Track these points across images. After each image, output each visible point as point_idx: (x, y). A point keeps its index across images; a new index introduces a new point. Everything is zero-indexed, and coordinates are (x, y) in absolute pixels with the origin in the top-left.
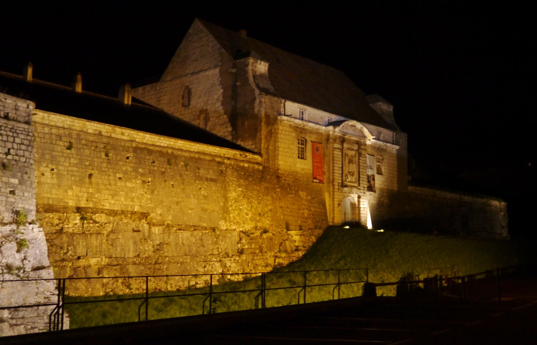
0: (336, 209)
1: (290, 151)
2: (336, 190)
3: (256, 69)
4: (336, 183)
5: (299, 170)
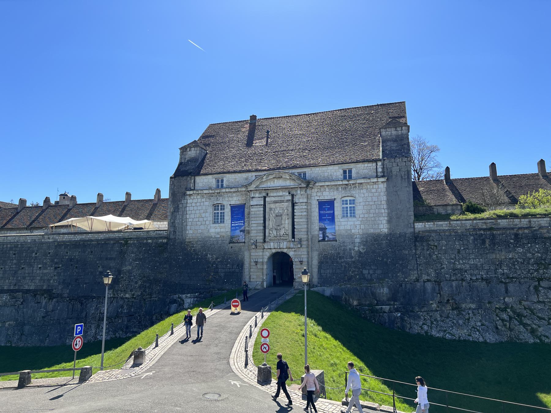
0: (252, 267)
1: (201, 219)
3: (187, 157)
5: (213, 235)
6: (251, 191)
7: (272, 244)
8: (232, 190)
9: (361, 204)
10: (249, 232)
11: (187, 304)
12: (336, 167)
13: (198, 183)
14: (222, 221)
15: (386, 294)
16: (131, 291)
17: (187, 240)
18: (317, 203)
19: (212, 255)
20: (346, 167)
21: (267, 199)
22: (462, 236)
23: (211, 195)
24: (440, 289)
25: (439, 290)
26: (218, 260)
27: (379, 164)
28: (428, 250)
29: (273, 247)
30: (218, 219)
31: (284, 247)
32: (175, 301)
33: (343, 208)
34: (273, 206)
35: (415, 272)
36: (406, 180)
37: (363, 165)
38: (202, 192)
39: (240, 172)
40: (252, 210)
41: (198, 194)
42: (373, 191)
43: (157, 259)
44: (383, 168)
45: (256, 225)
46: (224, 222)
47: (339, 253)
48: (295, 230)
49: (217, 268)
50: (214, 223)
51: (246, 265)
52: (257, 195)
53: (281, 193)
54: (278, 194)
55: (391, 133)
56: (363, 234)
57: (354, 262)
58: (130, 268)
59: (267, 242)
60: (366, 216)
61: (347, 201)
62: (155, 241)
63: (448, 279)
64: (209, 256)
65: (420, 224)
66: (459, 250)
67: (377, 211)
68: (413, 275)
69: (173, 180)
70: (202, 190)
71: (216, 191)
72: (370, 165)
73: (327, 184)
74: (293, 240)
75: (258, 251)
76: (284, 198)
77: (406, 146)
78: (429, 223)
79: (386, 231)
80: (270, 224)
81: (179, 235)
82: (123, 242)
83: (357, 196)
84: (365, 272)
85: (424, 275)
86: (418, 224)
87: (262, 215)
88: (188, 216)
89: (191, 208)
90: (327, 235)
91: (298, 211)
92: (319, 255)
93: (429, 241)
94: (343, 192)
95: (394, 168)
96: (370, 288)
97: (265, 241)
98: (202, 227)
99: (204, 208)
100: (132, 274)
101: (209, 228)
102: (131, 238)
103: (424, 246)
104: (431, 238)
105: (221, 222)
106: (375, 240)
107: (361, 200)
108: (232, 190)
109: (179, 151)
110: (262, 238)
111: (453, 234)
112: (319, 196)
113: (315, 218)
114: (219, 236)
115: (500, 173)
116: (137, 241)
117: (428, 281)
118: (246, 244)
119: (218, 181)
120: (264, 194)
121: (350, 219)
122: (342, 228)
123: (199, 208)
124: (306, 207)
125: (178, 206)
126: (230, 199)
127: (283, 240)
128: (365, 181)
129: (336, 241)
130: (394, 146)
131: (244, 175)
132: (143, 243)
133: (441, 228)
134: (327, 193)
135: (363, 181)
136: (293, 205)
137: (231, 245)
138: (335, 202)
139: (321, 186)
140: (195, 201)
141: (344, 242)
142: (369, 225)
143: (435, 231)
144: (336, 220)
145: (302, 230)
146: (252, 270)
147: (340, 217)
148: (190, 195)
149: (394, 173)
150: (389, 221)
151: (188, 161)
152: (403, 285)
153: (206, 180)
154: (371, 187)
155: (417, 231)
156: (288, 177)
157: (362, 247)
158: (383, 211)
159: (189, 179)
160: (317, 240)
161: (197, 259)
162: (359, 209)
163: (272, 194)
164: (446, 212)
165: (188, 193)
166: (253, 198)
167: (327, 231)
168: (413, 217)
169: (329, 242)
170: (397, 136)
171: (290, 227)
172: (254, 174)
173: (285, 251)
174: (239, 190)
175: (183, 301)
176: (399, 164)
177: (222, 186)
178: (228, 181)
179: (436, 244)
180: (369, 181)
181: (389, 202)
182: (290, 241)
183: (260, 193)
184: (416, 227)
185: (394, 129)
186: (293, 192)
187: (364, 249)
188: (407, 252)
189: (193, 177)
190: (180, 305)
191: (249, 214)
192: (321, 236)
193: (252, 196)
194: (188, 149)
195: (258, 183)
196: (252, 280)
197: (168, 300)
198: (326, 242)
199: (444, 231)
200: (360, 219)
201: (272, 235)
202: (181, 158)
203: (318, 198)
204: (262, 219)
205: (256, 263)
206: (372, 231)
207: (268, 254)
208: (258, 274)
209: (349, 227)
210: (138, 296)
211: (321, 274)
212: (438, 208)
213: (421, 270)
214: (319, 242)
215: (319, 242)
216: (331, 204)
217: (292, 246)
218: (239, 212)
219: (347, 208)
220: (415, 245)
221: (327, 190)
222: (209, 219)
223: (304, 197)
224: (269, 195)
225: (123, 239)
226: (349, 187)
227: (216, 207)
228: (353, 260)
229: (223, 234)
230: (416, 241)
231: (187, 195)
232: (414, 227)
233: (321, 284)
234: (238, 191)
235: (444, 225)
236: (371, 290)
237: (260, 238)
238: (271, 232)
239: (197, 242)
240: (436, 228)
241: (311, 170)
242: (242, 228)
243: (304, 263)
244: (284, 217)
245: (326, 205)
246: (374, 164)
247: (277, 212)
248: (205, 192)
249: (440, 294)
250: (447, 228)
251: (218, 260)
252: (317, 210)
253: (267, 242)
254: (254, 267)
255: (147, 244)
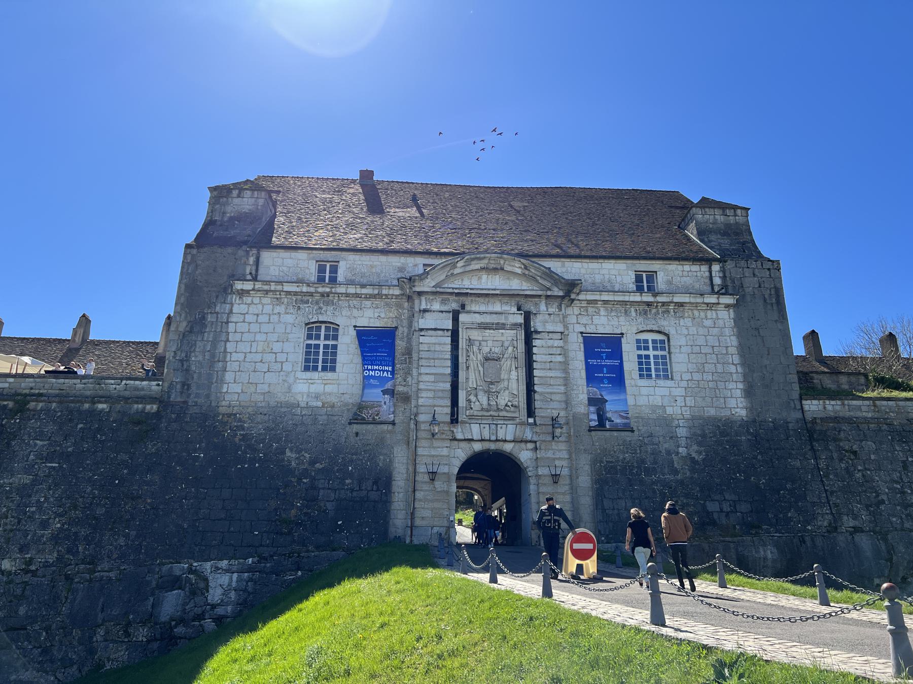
0: (418, 486)
1: (270, 357)
2: (422, 434)
3: (229, 209)
4: (421, 418)
5: (303, 400)
6: (420, 294)
7: (475, 428)
8: (364, 291)
9: (684, 349)
10: (406, 399)
11: (219, 591)
12: (621, 265)
13: (268, 267)
14: (330, 365)
15: (774, 561)
16: (23, 549)
17: (222, 410)
18: (581, 339)
19: (299, 451)
20: (644, 266)
21: (463, 318)
22: (904, 434)
23: (301, 299)
24: (891, 550)
25: (889, 552)
26: (318, 466)
27: (716, 267)
28: (841, 460)
29: (476, 435)
30: (319, 359)
31: (507, 436)
32: (175, 583)
33: (640, 357)
34: (475, 335)
35: (826, 510)
36: (775, 308)
37: (680, 267)
38: (279, 288)
39: (383, 252)
40: (422, 339)
41: (267, 292)
42: (708, 323)
43: (123, 456)
44: (724, 278)
45: (432, 378)
46: (333, 369)
47: (643, 461)
48: (537, 396)
49: (313, 487)
50: (307, 369)
51: (400, 483)
52: (436, 306)
53: (497, 307)
54: (490, 308)
55: (715, 219)
56: (693, 418)
57: (682, 482)
58: (27, 479)
59: (463, 422)
60: (697, 377)
61: (646, 341)
62: (118, 407)
63: (899, 527)
64: (288, 453)
65: (815, 402)
66: (903, 462)
67: (720, 368)
68: (823, 515)
69: (194, 251)
70: (280, 283)
71: (320, 290)
72: (695, 268)
73: (605, 297)
74: (531, 420)
75: (436, 443)
76: (506, 318)
77: (750, 245)
78: (833, 402)
79: (743, 413)
80: (470, 378)
81: (198, 396)
82: (11, 404)
83: (672, 332)
84: (712, 507)
85: (845, 518)
86: (809, 402)
87: (448, 356)
88: (230, 347)
89: (243, 327)
90: (609, 415)
91: (543, 351)
92: (594, 462)
93: (841, 440)
94: (640, 320)
95: (746, 280)
96: (732, 545)
97: (454, 420)
98: (271, 378)
99: (280, 329)
100: (34, 499)
101: (291, 379)
102: (41, 395)
103: (831, 451)
104: (842, 435)
105: (324, 369)
106: (723, 434)
107: (683, 341)
108: (364, 291)
109: (209, 194)
110: (448, 410)
111: (885, 427)
112: (585, 325)
113: (577, 374)
114: (320, 404)
115: (828, 350)
116: (60, 402)
117: (857, 530)
118: (398, 428)
119: (321, 269)
120: (455, 306)
121: (661, 382)
122: (642, 401)
123: (265, 328)
124: (561, 343)
125: (204, 317)
126: (355, 312)
127: (505, 418)
128: (692, 300)
129: (633, 431)
130: (726, 243)
131: (396, 261)
132: (80, 412)
133: (859, 414)
134: (603, 320)
135: (687, 300)
136: (529, 337)
137: (356, 428)
138: (624, 340)
139: (590, 302)
140: (253, 309)
141: (651, 435)
142: (704, 398)
143: (849, 420)
144: (627, 382)
145: (554, 397)
146: (419, 495)
147: (636, 374)
148: (242, 293)
149: (749, 290)
150: (749, 392)
151: (232, 219)
152: (807, 539)
153: (289, 262)
154: (702, 314)
155: (809, 417)
156: (519, 271)
157: (695, 447)
158: (733, 369)
159: (241, 253)
160: (585, 428)
161: (252, 461)
162: (680, 362)
163: (474, 307)
164: (839, 387)
165: (239, 285)
166: (425, 311)
167: (608, 407)
168: (796, 387)
169: (615, 434)
170: (728, 225)
171: (523, 388)
172: (421, 261)
173: (508, 447)
174: (385, 292)
175: (206, 580)
176: (757, 273)
177: (333, 280)
178: (351, 269)
179: (855, 447)
180: (699, 300)
181: (743, 350)
182: (522, 424)
183: (443, 302)
184: (806, 408)
185: (721, 212)
186: (529, 306)
187: (700, 453)
188: (798, 464)
189: (254, 251)
190: (193, 593)
191: (409, 352)
192: (595, 417)
193: (423, 307)
194: (235, 193)
195: (443, 277)
196: (418, 522)
197: (153, 579)
198: (608, 434)
199: (866, 421)
200: (684, 384)
201: (476, 406)
202: (211, 211)
203: (583, 330)
204: (449, 363)
205: (433, 475)
206: (712, 412)
207: (461, 454)
208: (437, 505)
209: (659, 399)
210: (46, 565)
211: (604, 510)
212: (820, 377)
213: (836, 505)
214: (590, 431)
215: (590, 431)
216: (613, 343)
217: (529, 435)
218: (377, 345)
219: (647, 357)
220: (812, 448)
221: (603, 312)
222: (291, 357)
223: (557, 319)
224: (468, 308)
225: (13, 395)
226: (654, 311)
227: (312, 330)
228: (679, 477)
229: (334, 399)
230: (811, 439)
231: (232, 293)
232: (802, 408)
233: (607, 537)
234: (379, 296)
235: (864, 408)
236: (737, 550)
237: (444, 412)
238: (473, 398)
239: (251, 417)
240: (848, 414)
241: (563, 266)
242: (389, 385)
243: (561, 481)
244: (506, 364)
245: (603, 345)
246: (705, 268)
247: (487, 350)
248: (288, 288)
249: (891, 560)
250: (870, 415)
251: (318, 466)
252: (581, 355)
253: (463, 422)
254: (425, 487)
255: (92, 413)
